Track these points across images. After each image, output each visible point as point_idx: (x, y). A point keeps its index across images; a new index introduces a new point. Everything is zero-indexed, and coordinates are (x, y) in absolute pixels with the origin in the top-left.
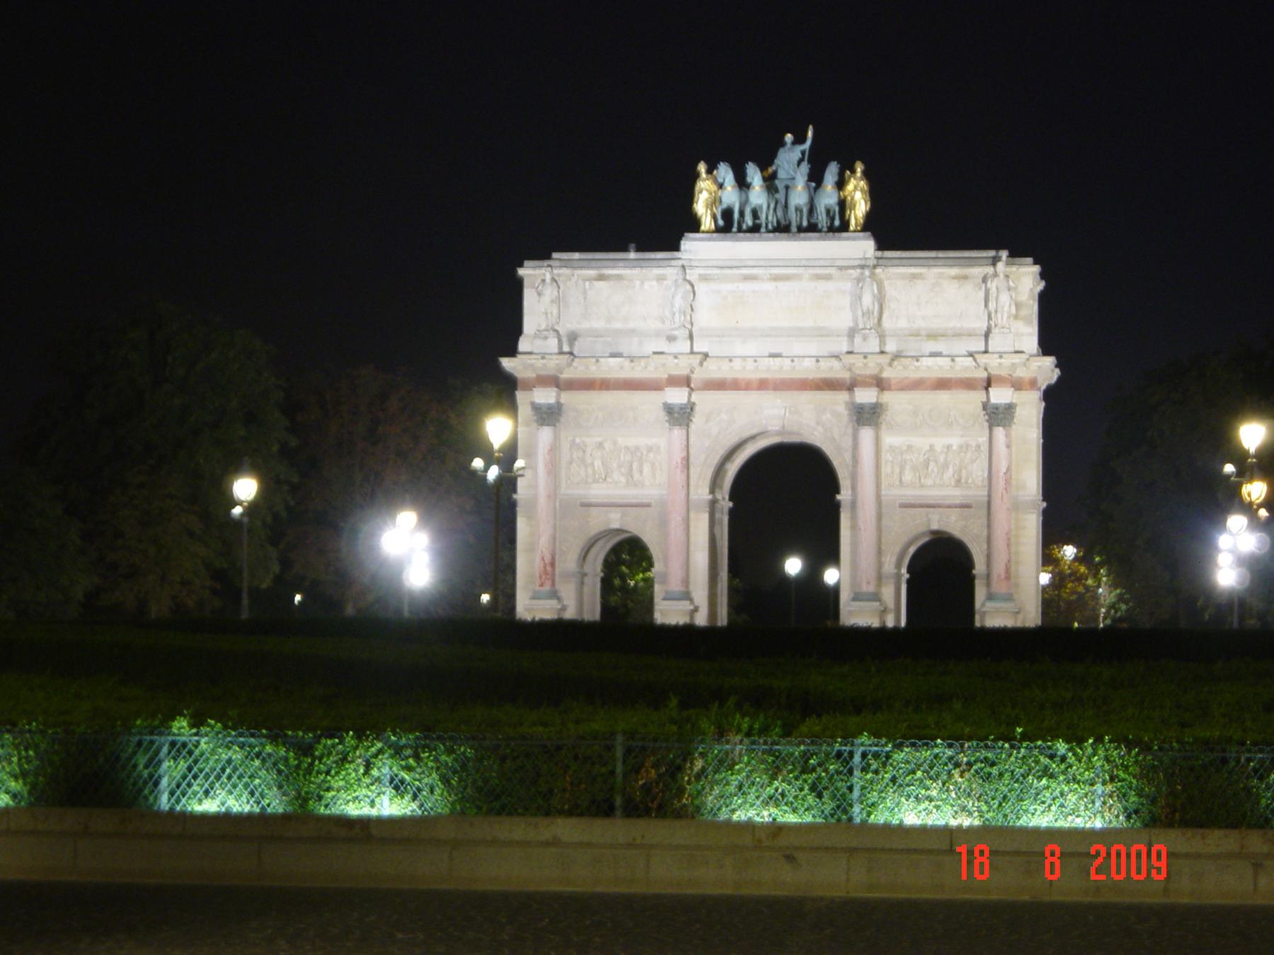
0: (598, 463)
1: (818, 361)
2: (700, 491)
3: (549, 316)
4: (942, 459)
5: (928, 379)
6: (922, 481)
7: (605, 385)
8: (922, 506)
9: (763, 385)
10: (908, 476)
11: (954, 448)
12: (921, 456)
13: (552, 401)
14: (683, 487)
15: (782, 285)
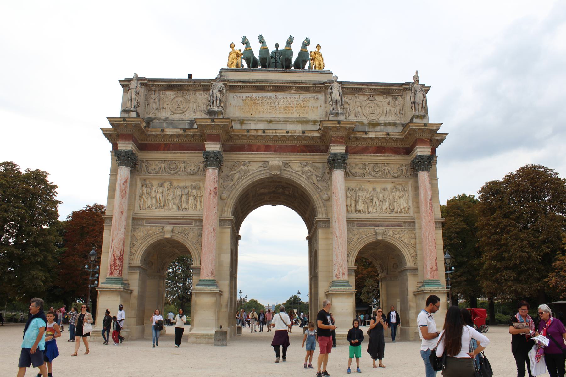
0: (159, 196)
1: (304, 132)
2: (225, 215)
3: (133, 101)
4: (381, 196)
5: (371, 147)
6: (370, 210)
7: (167, 147)
8: (370, 226)
9: (267, 149)
10: (360, 207)
11: (389, 189)
12: (368, 194)
13: (129, 149)
14: (214, 207)
15: (280, 95)
